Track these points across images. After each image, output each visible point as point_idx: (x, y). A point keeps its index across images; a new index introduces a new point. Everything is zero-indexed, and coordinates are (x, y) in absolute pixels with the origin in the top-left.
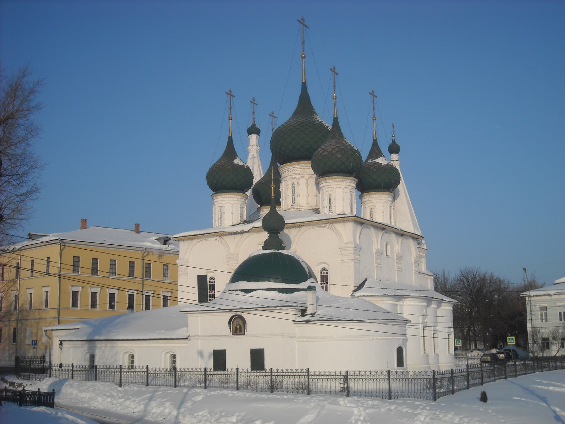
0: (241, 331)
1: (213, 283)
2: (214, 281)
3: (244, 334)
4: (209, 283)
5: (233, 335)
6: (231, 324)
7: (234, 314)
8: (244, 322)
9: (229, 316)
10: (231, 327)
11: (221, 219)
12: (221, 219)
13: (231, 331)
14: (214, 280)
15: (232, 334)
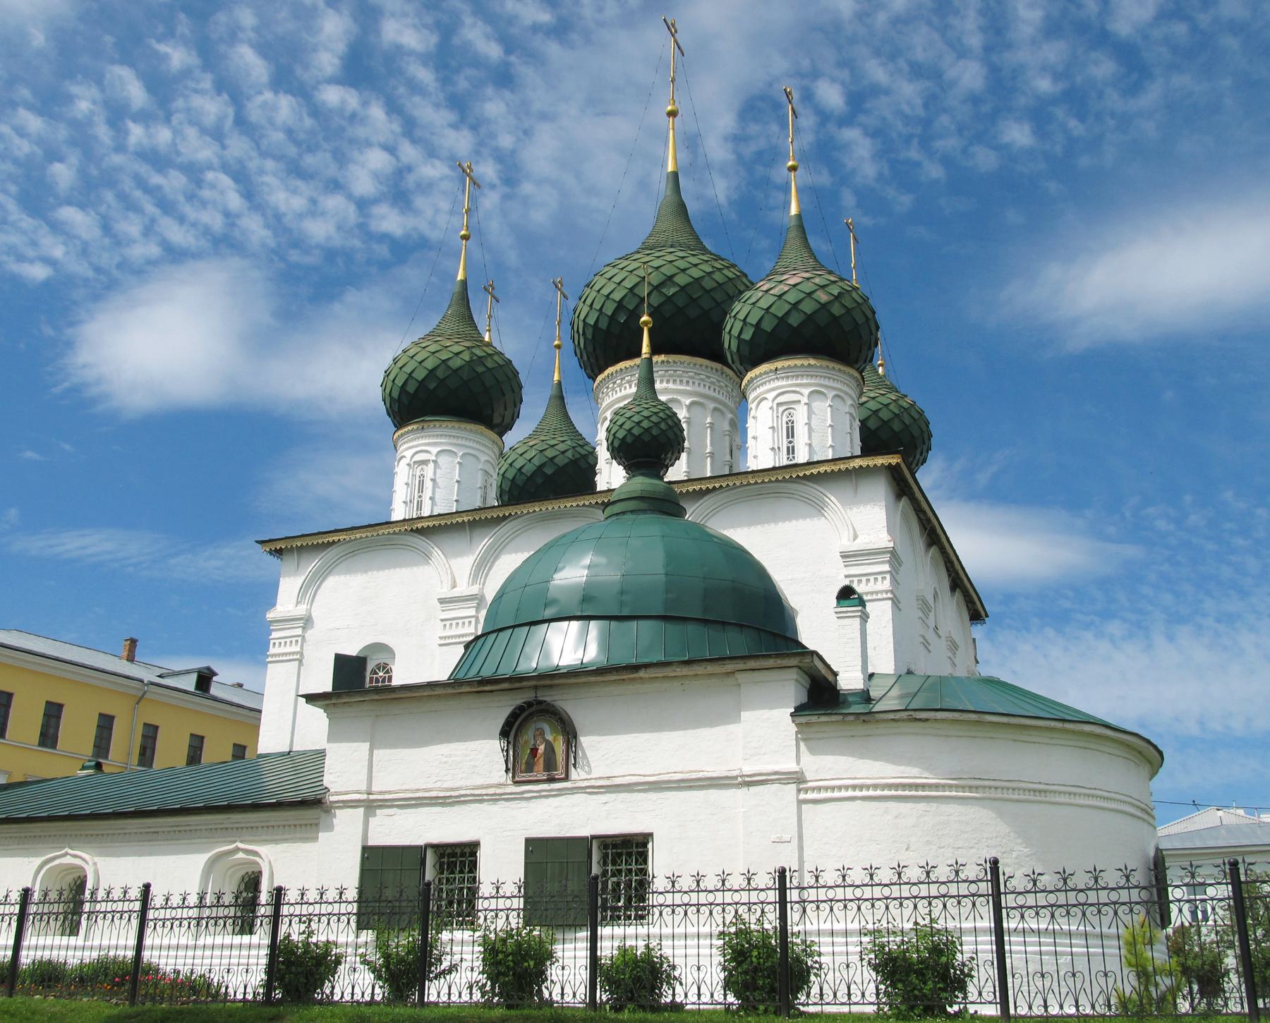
0: (550, 765)
1: (384, 681)
2: (387, 675)
3: (567, 778)
4: (371, 679)
5: (516, 783)
6: (511, 739)
7: (527, 696)
8: (570, 734)
9: (500, 712)
10: (507, 751)
11: (420, 497)
12: (420, 497)
13: (510, 766)
14: (387, 672)
15: (510, 782)
